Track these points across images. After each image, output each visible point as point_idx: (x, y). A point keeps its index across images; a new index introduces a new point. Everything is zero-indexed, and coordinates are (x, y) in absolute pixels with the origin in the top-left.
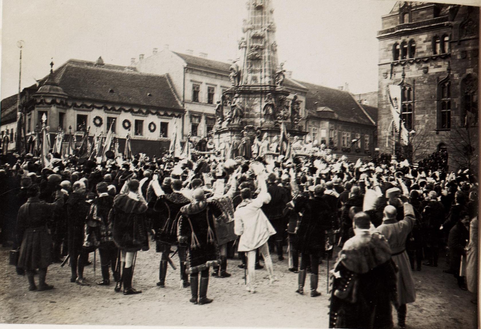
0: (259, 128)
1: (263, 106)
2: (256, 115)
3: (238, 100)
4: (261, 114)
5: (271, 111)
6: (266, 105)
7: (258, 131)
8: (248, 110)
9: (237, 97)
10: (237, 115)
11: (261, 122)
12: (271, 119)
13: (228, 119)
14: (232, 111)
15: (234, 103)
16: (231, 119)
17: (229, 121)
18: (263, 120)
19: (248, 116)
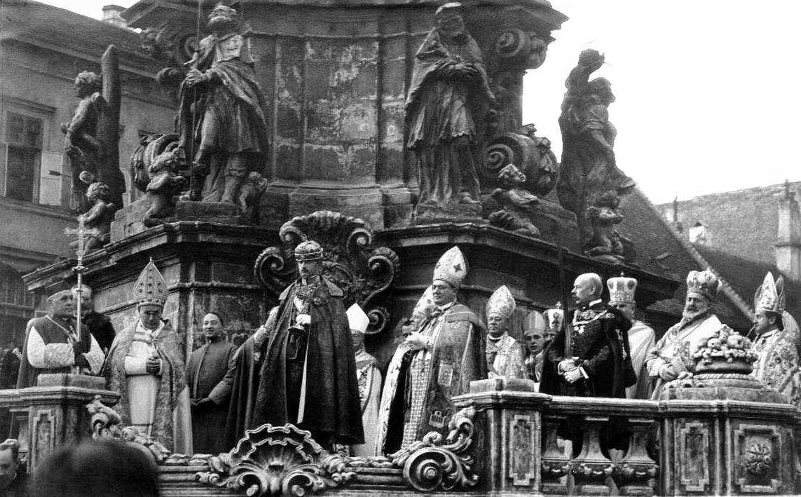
0: (382, 238)
1: (397, 103)
2: (345, 158)
3: (234, 45)
4: (382, 154)
5: (461, 122)
6: (431, 80)
7: (382, 253)
8: (291, 125)
9: (223, 29)
10: (219, 152)
11: (386, 199)
12: (461, 180)
13: (157, 181)
14: (191, 120)
15: (204, 66)
16: (187, 175)
17: (168, 192)
18: (398, 191)
19: (293, 170)
